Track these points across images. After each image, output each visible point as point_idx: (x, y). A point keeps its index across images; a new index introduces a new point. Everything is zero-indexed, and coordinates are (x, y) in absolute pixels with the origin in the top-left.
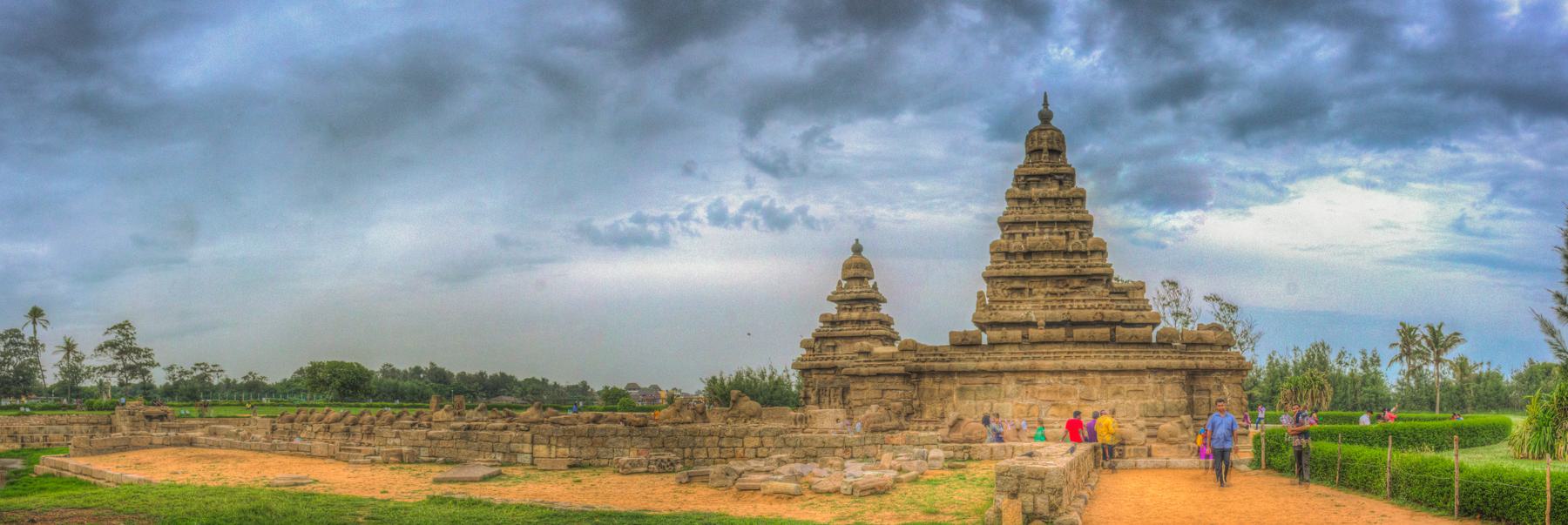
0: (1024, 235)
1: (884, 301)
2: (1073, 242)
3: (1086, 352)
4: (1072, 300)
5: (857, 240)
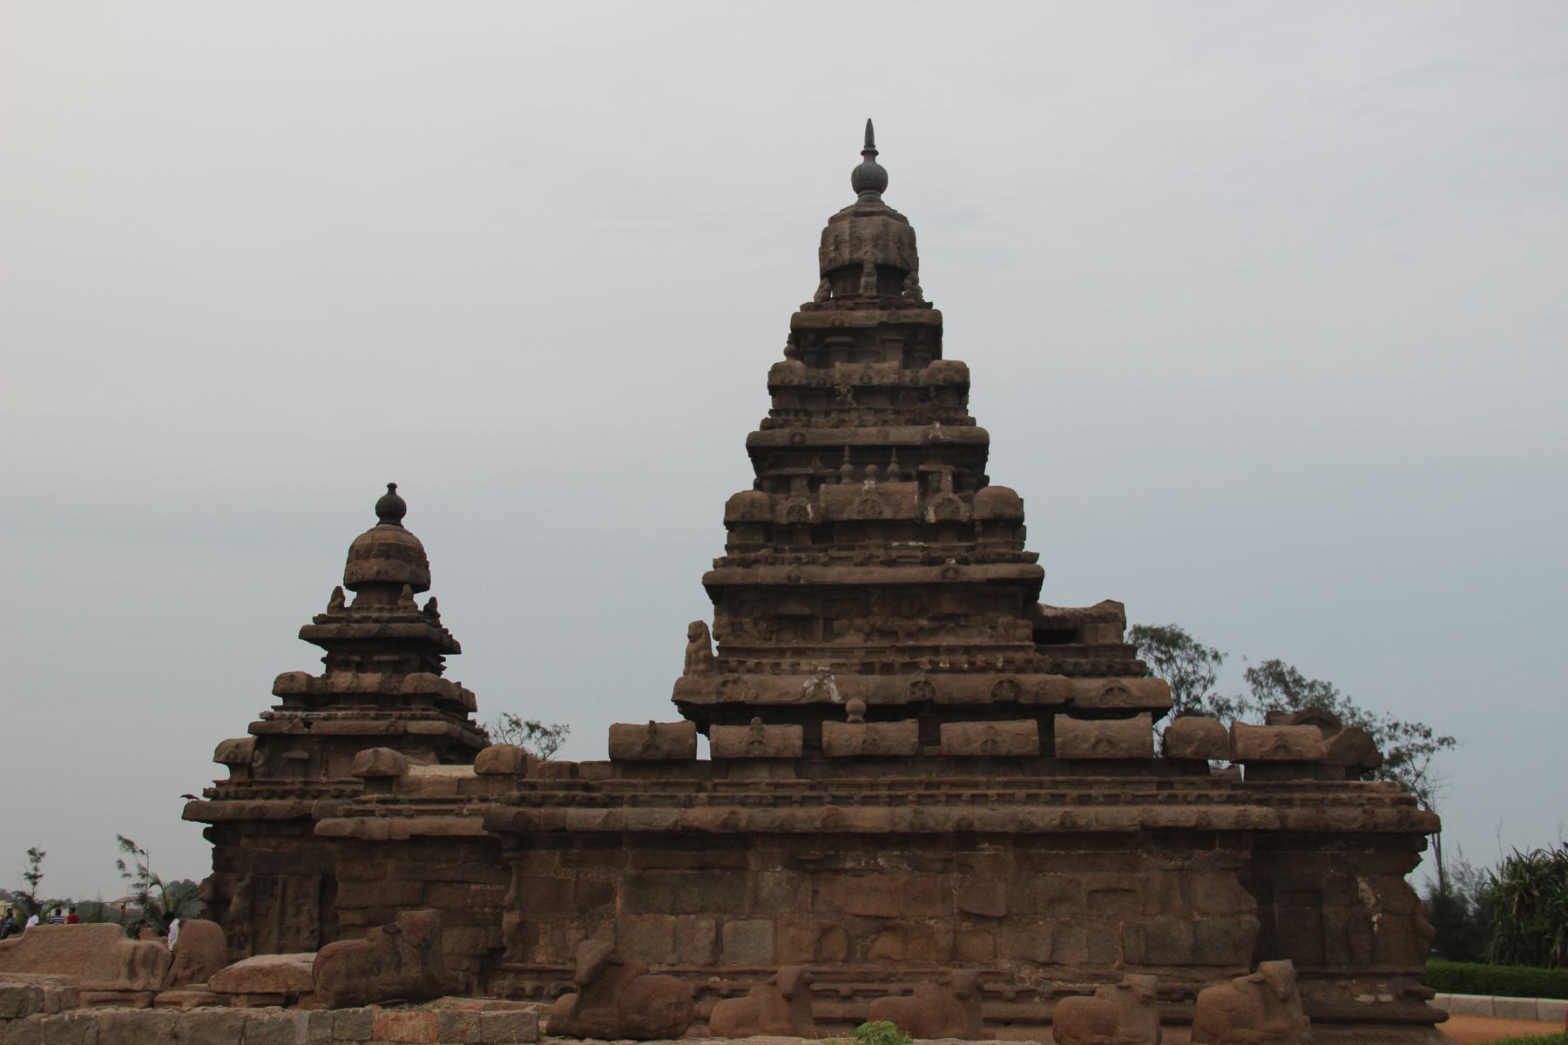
0: (814, 482)
1: (454, 648)
2: (938, 498)
3: (976, 785)
4: (936, 650)
5: (392, 487)
